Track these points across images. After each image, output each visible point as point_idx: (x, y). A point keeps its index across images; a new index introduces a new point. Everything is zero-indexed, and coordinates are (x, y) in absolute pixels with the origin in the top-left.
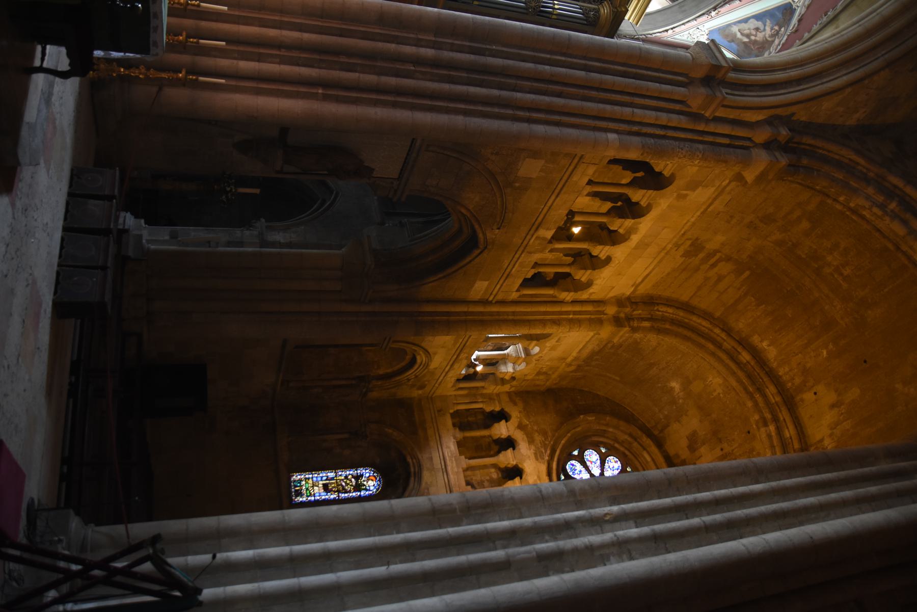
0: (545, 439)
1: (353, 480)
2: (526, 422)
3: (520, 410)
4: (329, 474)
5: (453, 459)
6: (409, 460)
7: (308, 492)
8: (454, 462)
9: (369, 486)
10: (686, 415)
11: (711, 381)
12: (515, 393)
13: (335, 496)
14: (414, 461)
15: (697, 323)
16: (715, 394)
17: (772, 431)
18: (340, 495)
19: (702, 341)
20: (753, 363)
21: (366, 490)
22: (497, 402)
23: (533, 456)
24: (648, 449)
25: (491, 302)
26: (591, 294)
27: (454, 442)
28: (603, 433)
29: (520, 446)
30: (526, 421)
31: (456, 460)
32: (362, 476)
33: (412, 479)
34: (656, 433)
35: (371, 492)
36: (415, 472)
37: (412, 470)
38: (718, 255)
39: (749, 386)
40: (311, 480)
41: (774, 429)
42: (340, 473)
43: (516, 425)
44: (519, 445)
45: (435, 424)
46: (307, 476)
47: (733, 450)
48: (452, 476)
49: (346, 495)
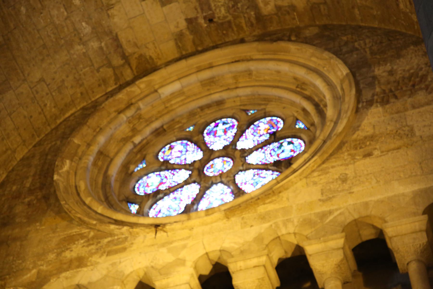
23: (115, 258)
30: (29, 275)
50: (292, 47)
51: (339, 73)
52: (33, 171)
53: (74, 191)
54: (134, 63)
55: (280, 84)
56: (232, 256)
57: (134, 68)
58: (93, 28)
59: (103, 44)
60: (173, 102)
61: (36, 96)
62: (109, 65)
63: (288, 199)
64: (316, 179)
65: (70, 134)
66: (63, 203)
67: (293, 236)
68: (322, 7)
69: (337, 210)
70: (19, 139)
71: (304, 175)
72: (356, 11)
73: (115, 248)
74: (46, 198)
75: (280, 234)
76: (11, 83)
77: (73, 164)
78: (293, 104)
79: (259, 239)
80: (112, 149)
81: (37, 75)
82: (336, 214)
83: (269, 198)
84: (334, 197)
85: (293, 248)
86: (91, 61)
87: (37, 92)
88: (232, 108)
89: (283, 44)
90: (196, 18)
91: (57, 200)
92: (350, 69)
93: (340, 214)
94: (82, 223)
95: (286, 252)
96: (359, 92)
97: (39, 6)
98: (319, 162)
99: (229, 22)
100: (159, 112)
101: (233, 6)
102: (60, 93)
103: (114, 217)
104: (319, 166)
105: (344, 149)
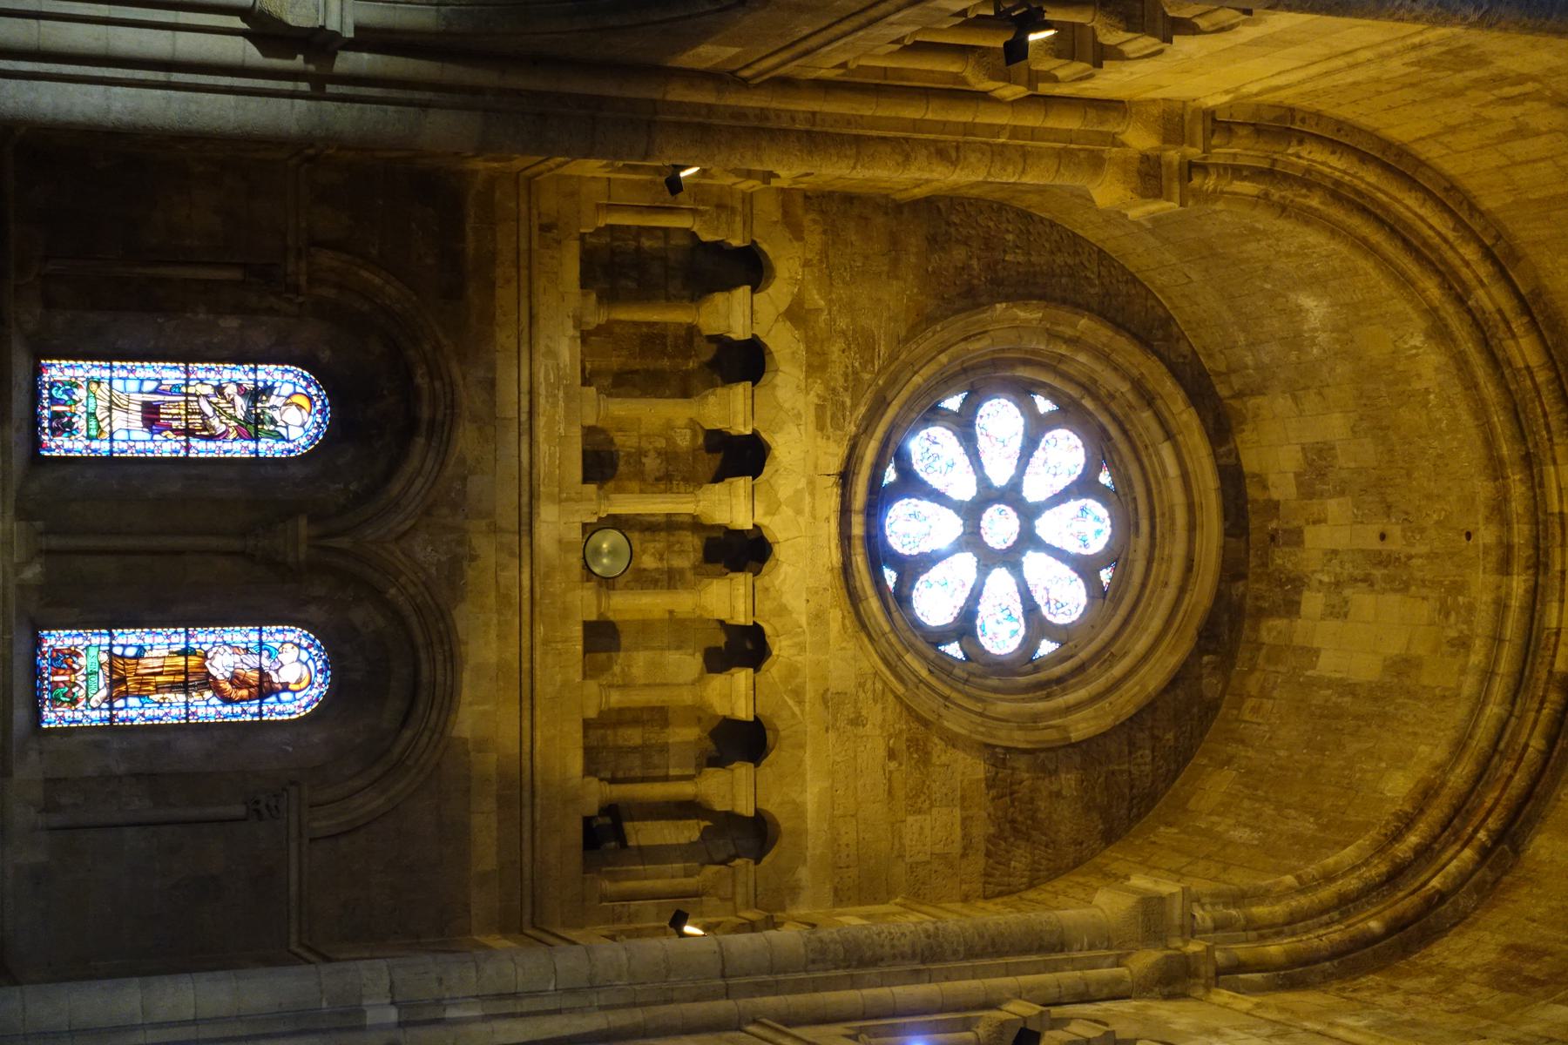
0: (864, 366)
1: (239, 401)
2: (816, 299)
3: (809, 256)
4: (166, 373)
5: (561, 394)
6: (421, 380)
7: (93, 423)
8: (561, 403)
10: (1320, 394)
11: (1415, 347)
12: (807, 197)
13: (177, 446)
14: (438, 384)
15: (1416, 214)
16: (1418, 385)
17: (1514, 594)
18: (193, 442)
19: (1413, 269)
20: (1541, 377)
22: (738, 219)
23: (810, 416)
24: (1180, 438)
25: (745, 81)
26: (1086, 89)
27: (573, 338)
28: (1051, 365)
29: (779, 379)
31: (569, 398)
32: (268, 390)
33: (421, 441)
34: (1223, 391)
35: (291, 446)
36: (432, 422)
38: (1529, 87)
39: (1503, 441)
40: (105, 386)
41: (1521, 591)
42: (201, 375)
43: (782, 309)
44: (777, 370)
45: (524, 272)
46: (95, 373)
47: (1410, 557)
48: (543, 448)
49: (211, 445)
57: (1231, 402)
69: (802, 711)
72: (1205, 761)
77: (1034, 323)
82: (796, 710)
93: (794, 715)
94: (893, 357)
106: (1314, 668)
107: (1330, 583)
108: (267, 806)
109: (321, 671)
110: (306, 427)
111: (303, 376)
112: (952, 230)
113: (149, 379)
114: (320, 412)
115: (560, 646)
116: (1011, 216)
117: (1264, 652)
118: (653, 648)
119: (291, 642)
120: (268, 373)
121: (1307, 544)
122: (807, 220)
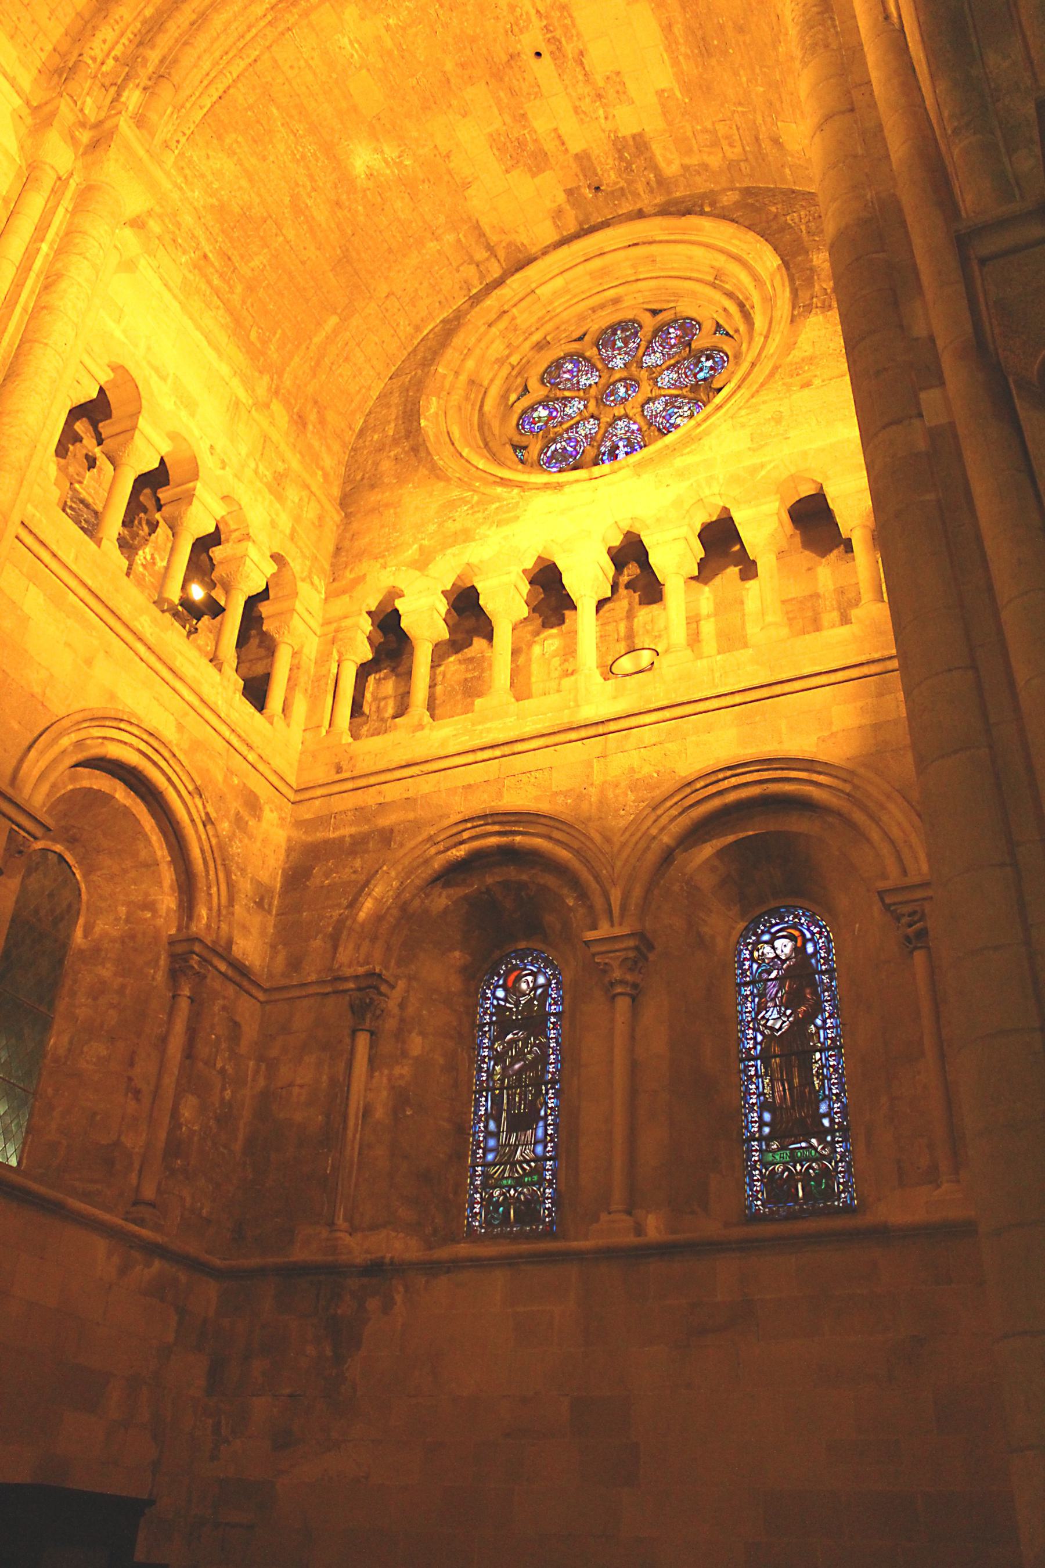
0: (466, 503)
3: (379, 566)
6: (460, 852)
8: (488, 725)
9: (535, 988)
14: (466, 835)
21: (546, 995)
23: (506, 530)
29: (474, 560)
30: (410, 552)
37: (493, 840)
43: (418, 573)
50: (707, 224)
51: (769, 264)
52: (394, 411)
53: (447, 439)
54: (501, 254)
55: (695, 275)
56: (648, 527)
57: (502, 260)
58: (447, 217)
59: (461, 236)
60: (556, 304)
61: (387, 315)
62: (471, 261)
63: (711, 448)
64: (743, 420)
65: (433, 359)
66: (436, 458)
67: (718, 498)
68: (742, 164)
69: (770, 462)
70: (372, 373)
71: (730, 414)
72: (787, 171)
73: (505, 516)
74: (415, 450)
75: (702, 496)
76: (356, 304)
78: (710, 301)
79: (678, 503)
80: (486, 376)
81: (383, 289)
82: (769, 467)
83: (687, 447)
84: (766, 444)
85: (719, 510)
86: (448, 259)
87: (387, 310)
88: (632, 307)
89: (693, 220)
90: (578, 188)
91: (429, 453)
92: (782, 259)
93: (775, 467)
95: (710, 515)
96: (795, 292)
97: (379, 199)
98: (748, 395)
99: (622, 189)
100: (540, 319)
101: (626, 168)
102: (414, 306)
103: (500, 475)
104: (748, 401)
105: (777, 376)
106: (672, 90)
107: (604, 106)
108: (910, 925)
109: (782, 919)
110: (535, 970)
111: (488, 980)
112: (367, 476)
113: (486, 1127)
114: (522, 961)
115: (717, 675)
116: (361, 441)
117: (687, 161)
118: (744, 623)
119: (751, 953)
120: (485, 1013)
121: (584, 146)
122: (350, 576)
